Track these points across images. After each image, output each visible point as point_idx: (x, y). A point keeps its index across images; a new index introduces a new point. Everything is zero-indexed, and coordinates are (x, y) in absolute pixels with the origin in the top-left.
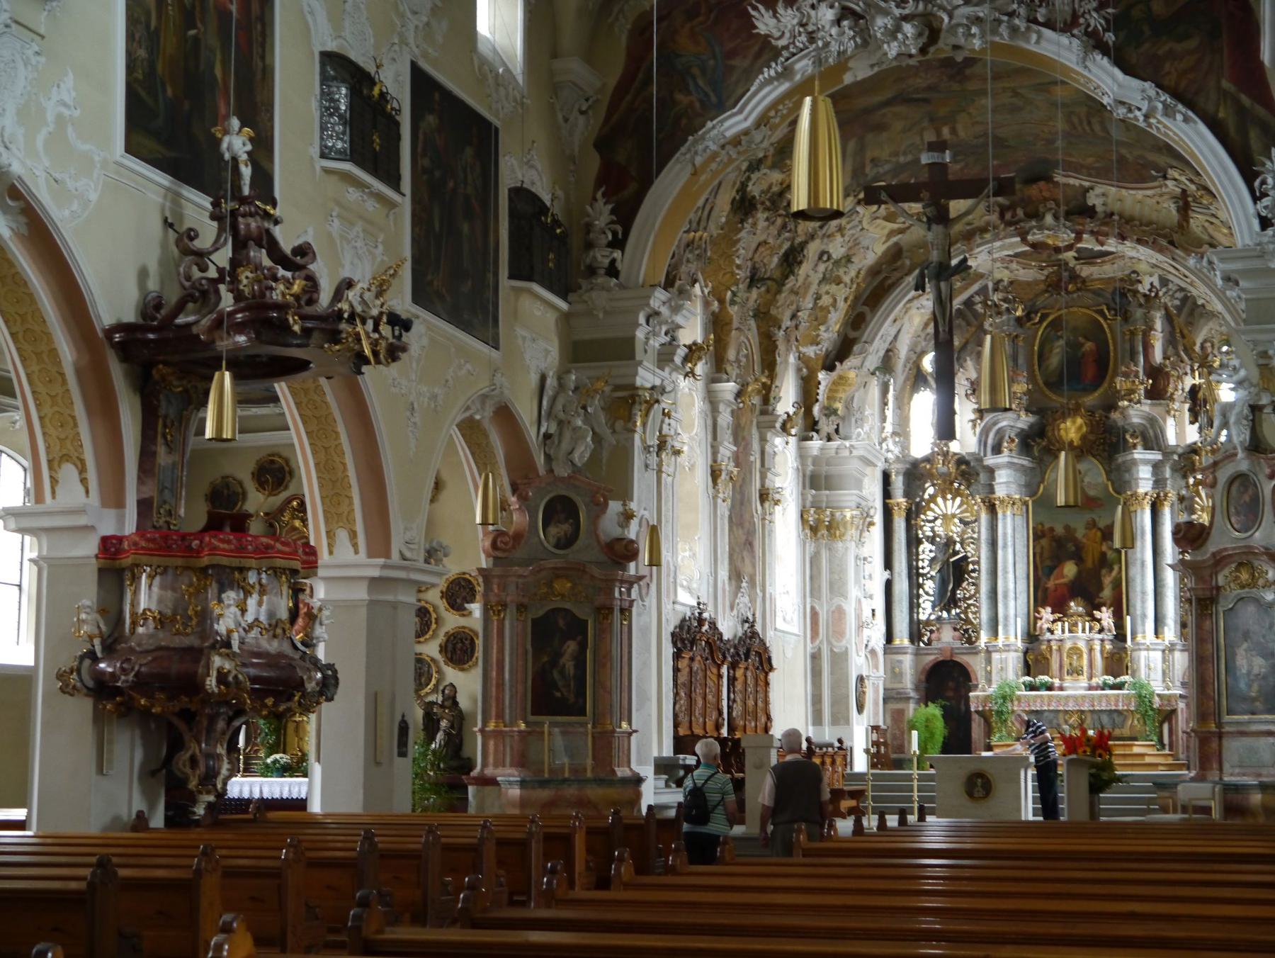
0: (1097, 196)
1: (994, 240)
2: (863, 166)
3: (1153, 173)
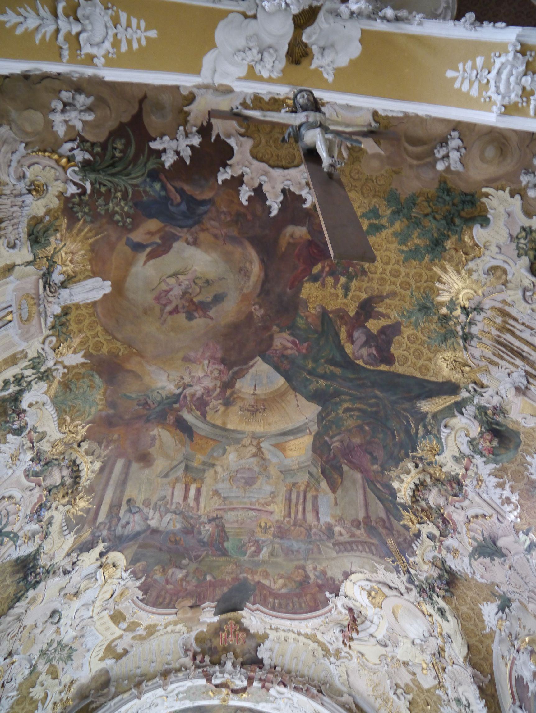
0: (266, 650)
1: (185, 680)
2: (119, 506)
3: (327, 593)
